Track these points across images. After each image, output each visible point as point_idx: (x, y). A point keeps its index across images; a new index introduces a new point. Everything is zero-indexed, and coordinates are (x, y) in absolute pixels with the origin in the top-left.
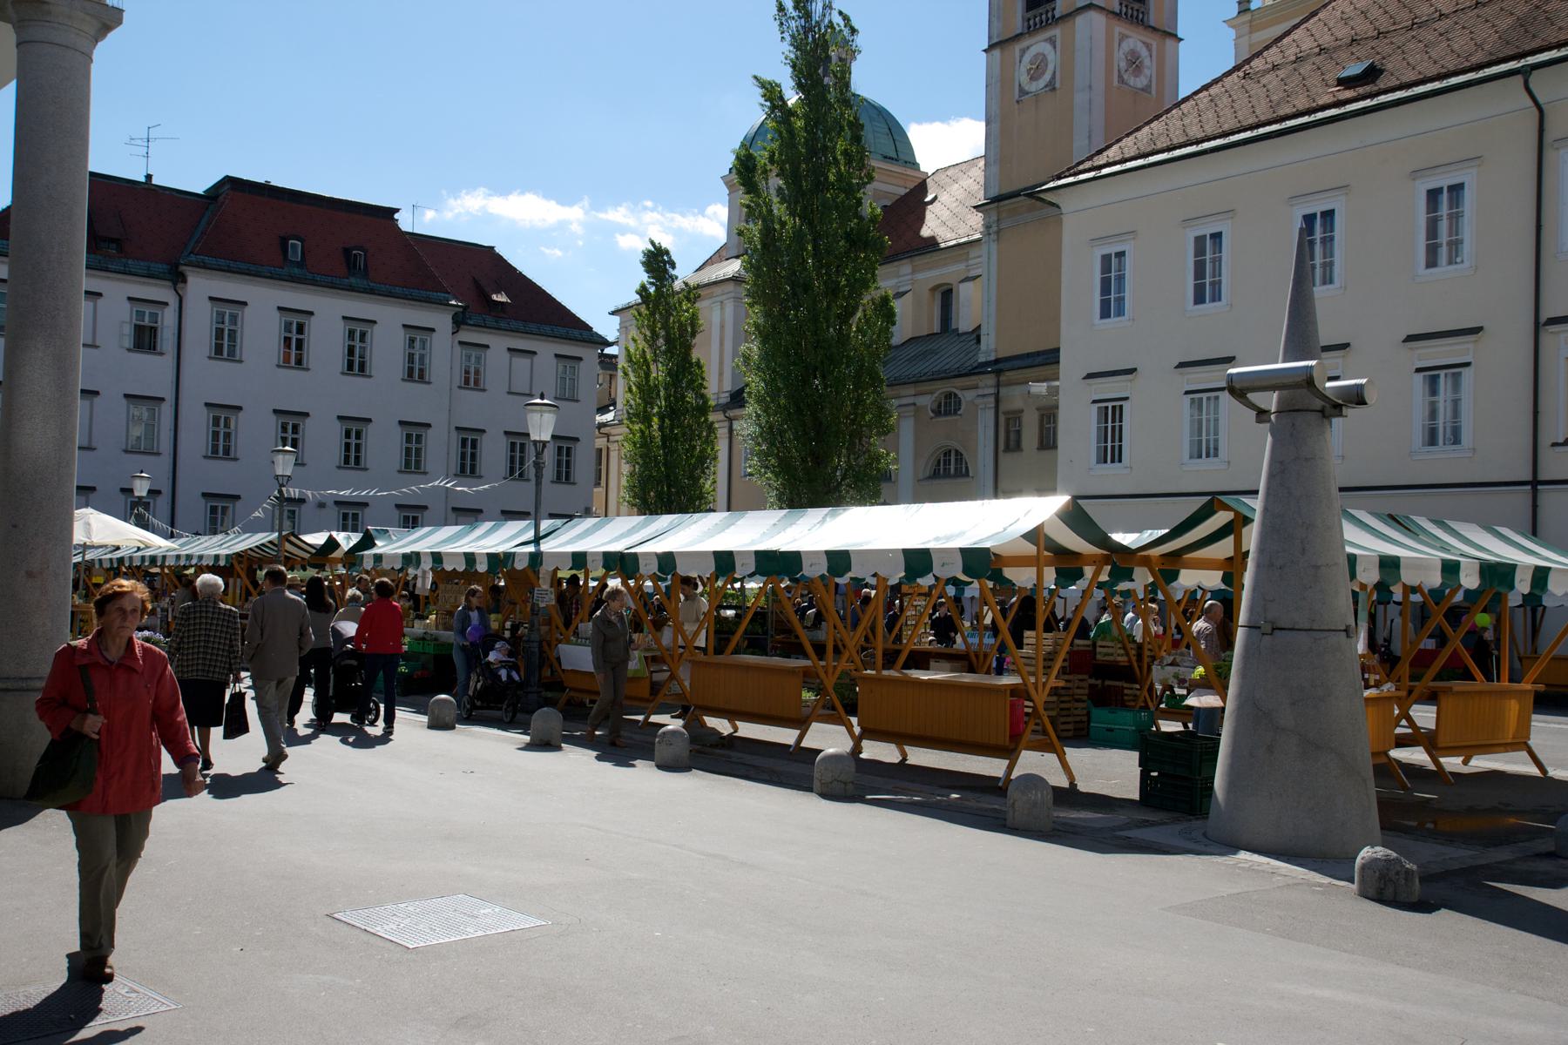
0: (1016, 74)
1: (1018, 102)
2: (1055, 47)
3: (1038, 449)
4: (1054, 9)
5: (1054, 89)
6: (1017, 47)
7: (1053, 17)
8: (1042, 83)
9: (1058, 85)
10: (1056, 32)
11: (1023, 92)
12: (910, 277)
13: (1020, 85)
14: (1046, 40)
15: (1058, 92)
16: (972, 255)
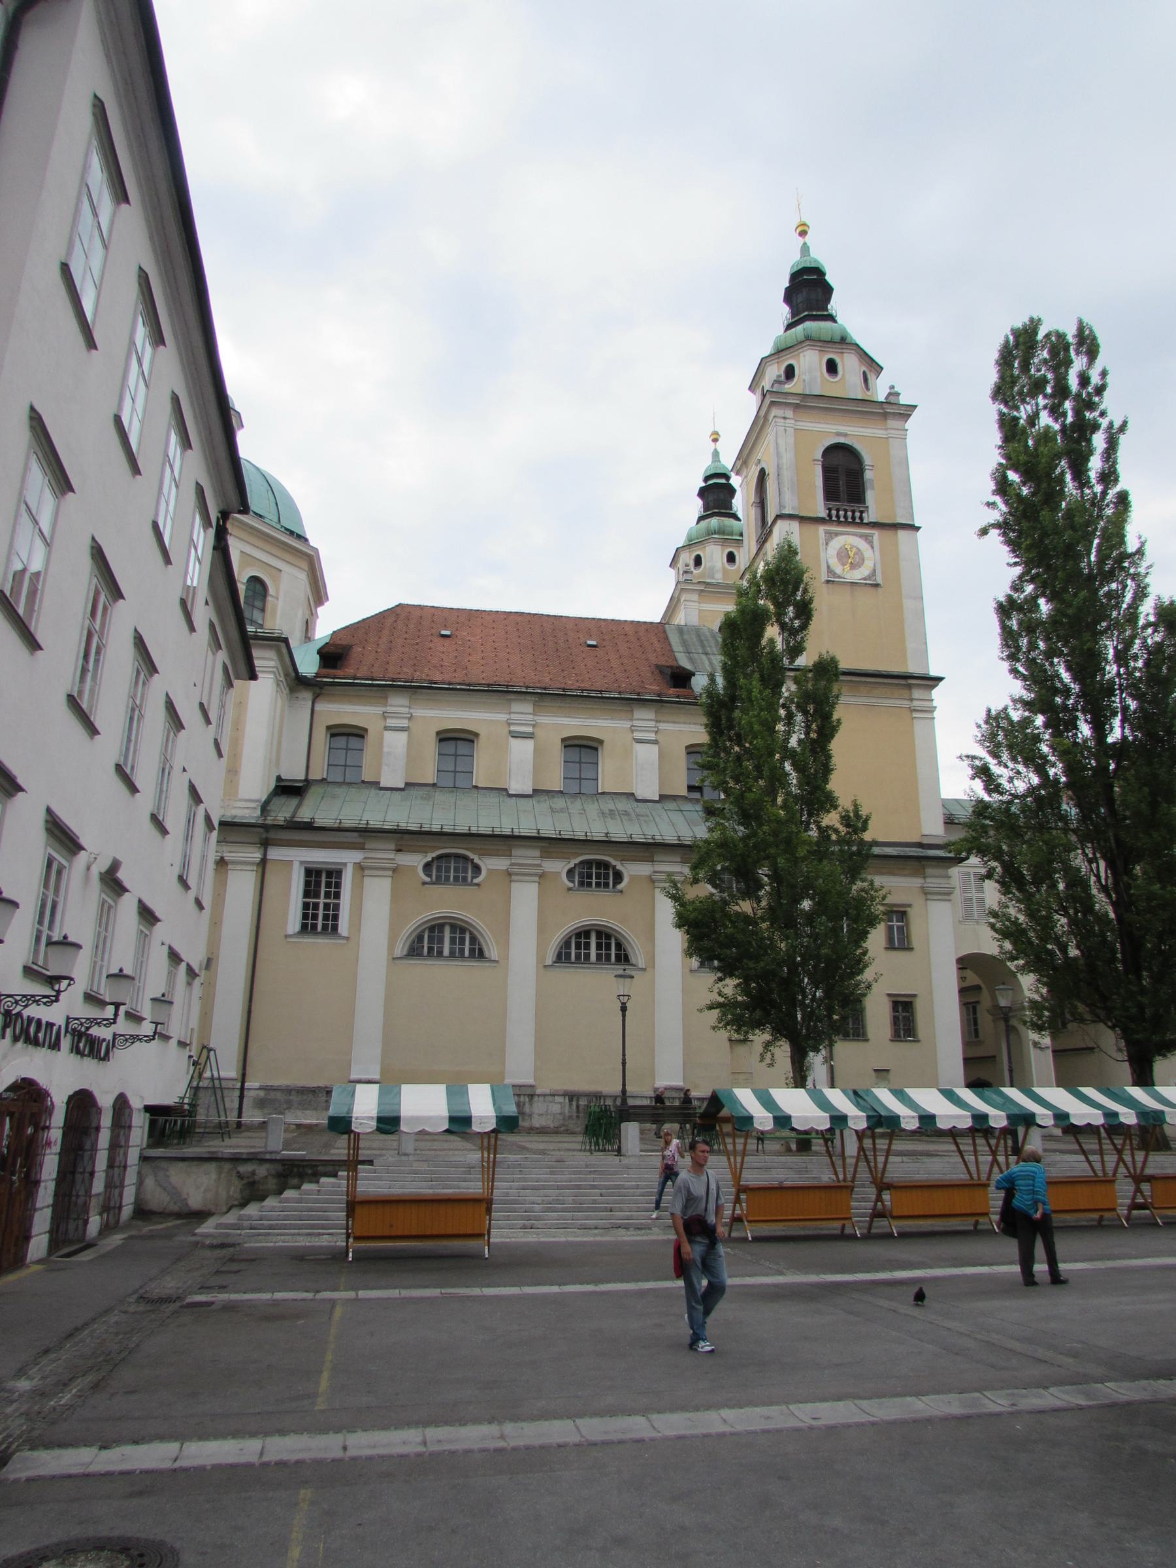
0: (822, 555)
1: (828, 582)
2: (873, 547)
3: (887, 948)
4: (862, 512)
5: (877, 585)
6: (822, 529)
7: (861, 518)
8: (857, 575)
9: (879, 581)
10: (876, 534)
11: (830, 570)
12: (531, 716)
13: (828, 567)
14: (861, 536)
15: (880, 589)
16: (636, 716)
